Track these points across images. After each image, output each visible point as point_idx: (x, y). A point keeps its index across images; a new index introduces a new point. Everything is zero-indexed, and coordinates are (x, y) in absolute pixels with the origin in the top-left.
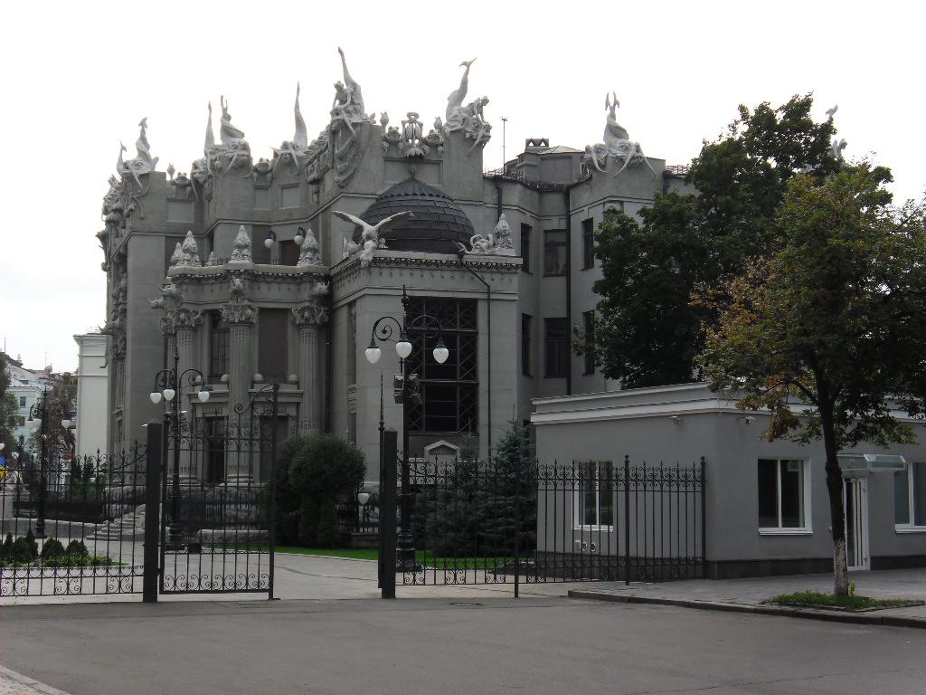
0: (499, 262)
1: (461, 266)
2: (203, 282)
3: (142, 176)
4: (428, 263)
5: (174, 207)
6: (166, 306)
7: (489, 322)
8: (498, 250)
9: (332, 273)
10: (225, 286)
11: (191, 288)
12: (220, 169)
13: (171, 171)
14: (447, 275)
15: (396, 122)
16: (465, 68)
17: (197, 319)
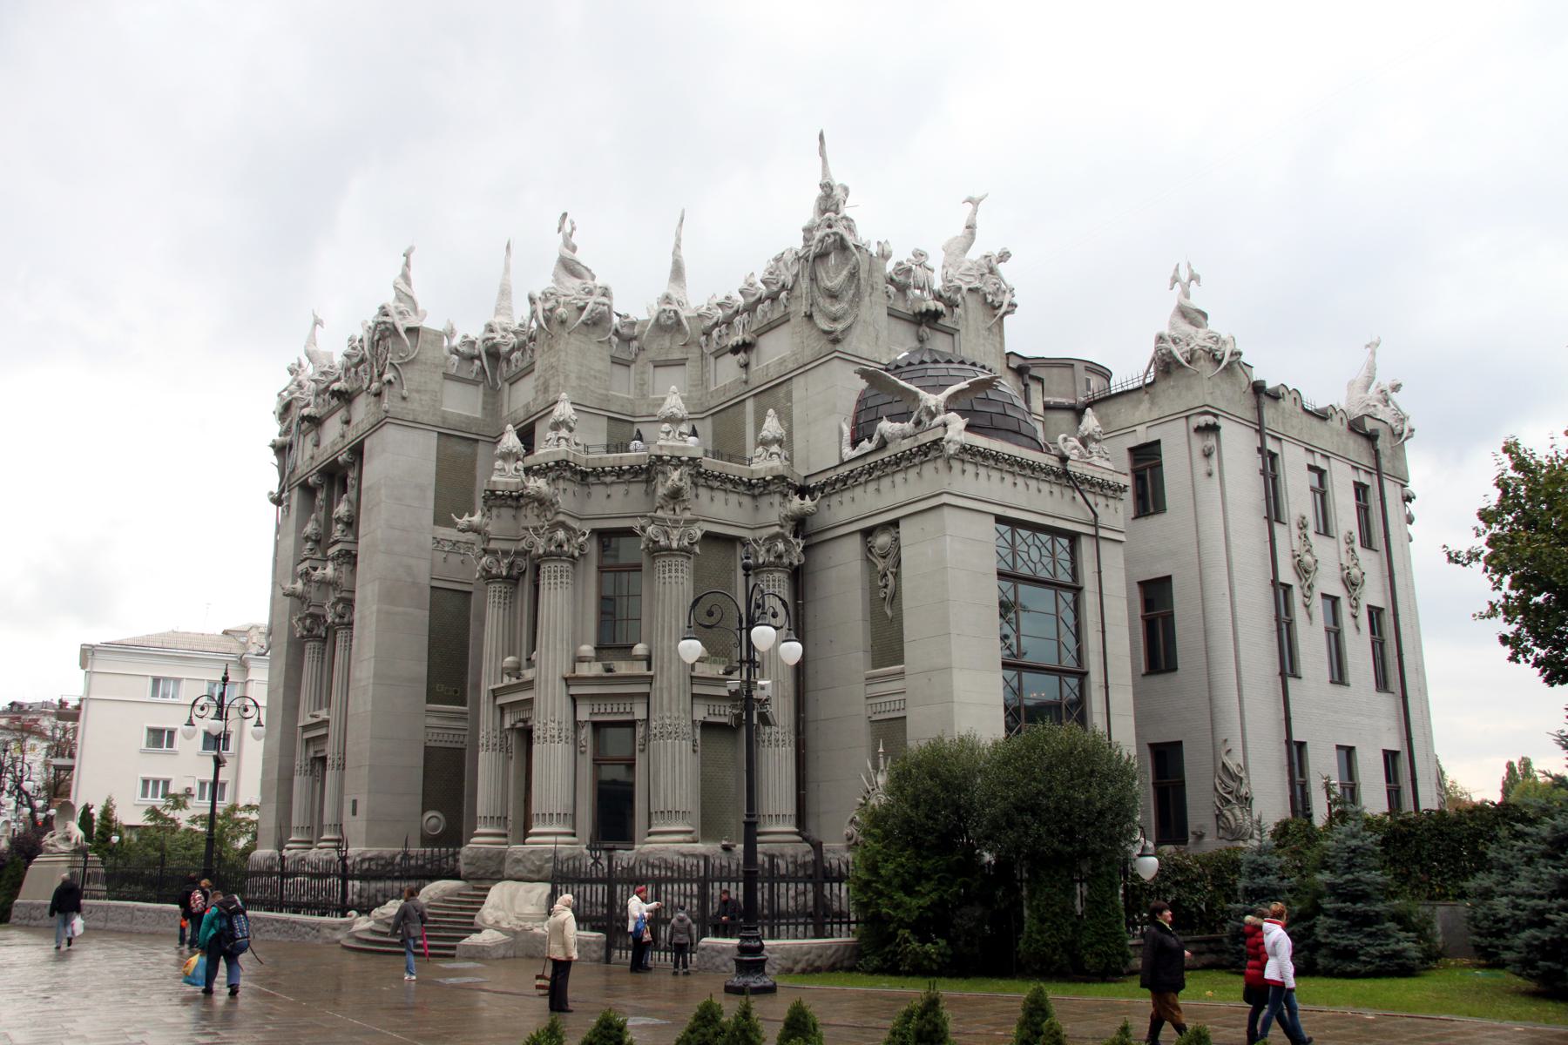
0: (1106, 477)
1: (1064, 477)
2: (591, 479)
3: (409, 331)
4: (1022, 464)
5: (453, 388)
6: (489, 529)
7: (1099, 572)
8: (1095, 460)
9: (812, 483)
10: (637, 490)
11: (571, 487)
12: (563, 322)
13: (451, 334)
14: (1045, 487)
15: (901, 254)
16: (969, 206)
17: (581, 547)
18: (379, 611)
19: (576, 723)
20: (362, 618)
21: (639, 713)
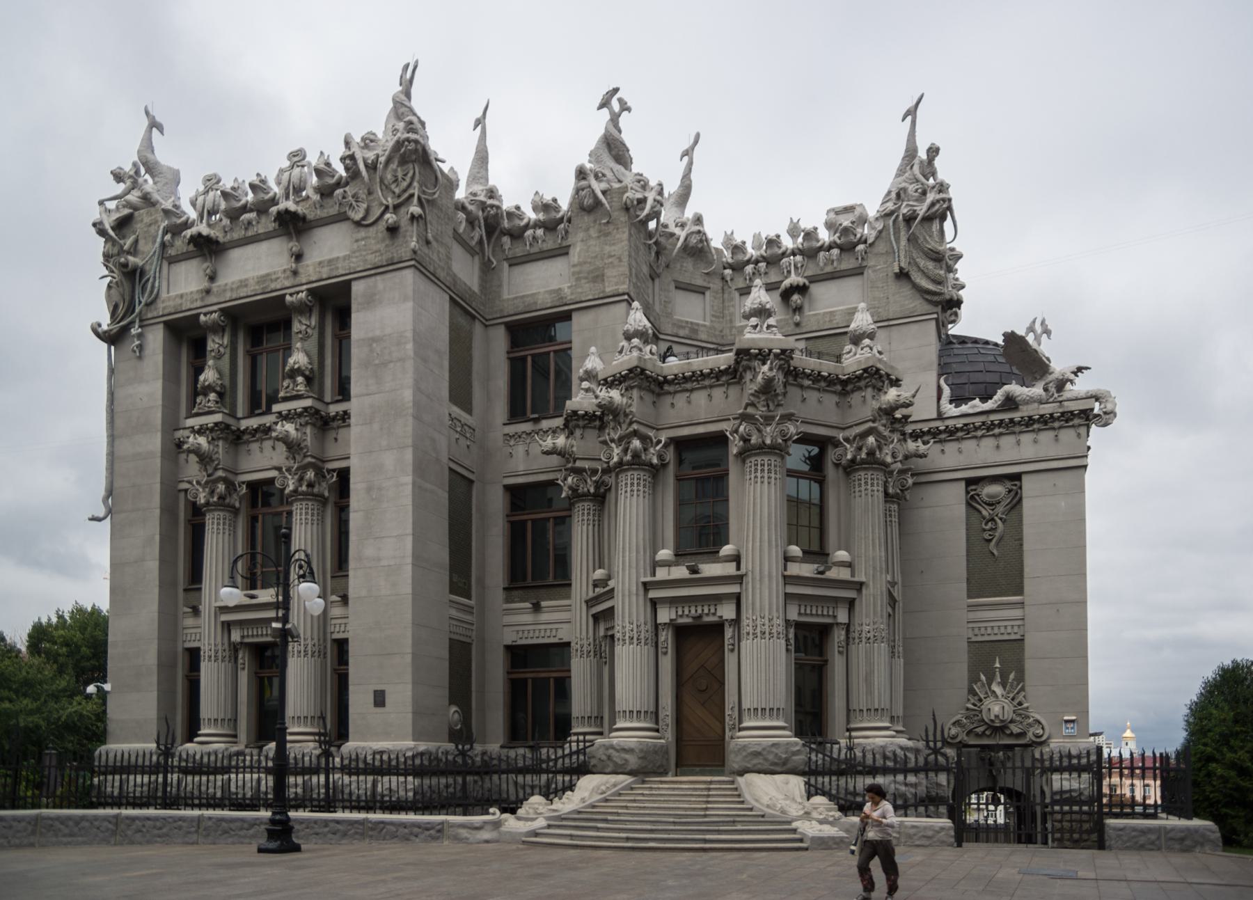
6: (634, 409)
18: (414, 484)
19: (787, 621)
20: (369, 490)
21: (842, 617)
